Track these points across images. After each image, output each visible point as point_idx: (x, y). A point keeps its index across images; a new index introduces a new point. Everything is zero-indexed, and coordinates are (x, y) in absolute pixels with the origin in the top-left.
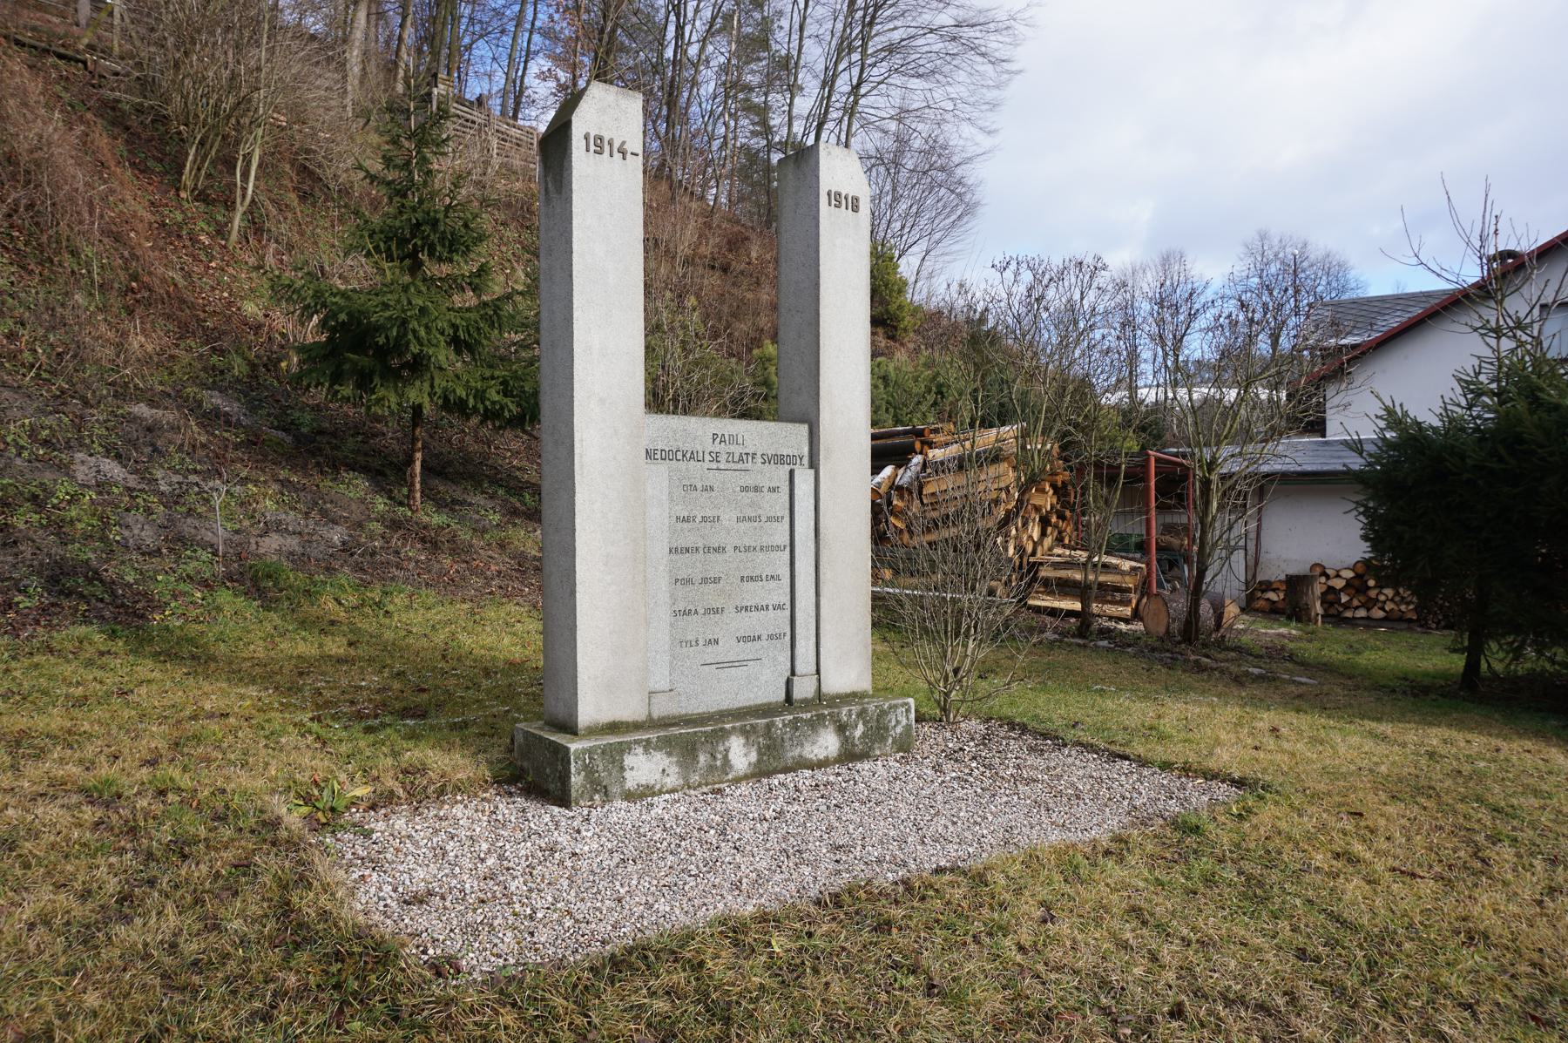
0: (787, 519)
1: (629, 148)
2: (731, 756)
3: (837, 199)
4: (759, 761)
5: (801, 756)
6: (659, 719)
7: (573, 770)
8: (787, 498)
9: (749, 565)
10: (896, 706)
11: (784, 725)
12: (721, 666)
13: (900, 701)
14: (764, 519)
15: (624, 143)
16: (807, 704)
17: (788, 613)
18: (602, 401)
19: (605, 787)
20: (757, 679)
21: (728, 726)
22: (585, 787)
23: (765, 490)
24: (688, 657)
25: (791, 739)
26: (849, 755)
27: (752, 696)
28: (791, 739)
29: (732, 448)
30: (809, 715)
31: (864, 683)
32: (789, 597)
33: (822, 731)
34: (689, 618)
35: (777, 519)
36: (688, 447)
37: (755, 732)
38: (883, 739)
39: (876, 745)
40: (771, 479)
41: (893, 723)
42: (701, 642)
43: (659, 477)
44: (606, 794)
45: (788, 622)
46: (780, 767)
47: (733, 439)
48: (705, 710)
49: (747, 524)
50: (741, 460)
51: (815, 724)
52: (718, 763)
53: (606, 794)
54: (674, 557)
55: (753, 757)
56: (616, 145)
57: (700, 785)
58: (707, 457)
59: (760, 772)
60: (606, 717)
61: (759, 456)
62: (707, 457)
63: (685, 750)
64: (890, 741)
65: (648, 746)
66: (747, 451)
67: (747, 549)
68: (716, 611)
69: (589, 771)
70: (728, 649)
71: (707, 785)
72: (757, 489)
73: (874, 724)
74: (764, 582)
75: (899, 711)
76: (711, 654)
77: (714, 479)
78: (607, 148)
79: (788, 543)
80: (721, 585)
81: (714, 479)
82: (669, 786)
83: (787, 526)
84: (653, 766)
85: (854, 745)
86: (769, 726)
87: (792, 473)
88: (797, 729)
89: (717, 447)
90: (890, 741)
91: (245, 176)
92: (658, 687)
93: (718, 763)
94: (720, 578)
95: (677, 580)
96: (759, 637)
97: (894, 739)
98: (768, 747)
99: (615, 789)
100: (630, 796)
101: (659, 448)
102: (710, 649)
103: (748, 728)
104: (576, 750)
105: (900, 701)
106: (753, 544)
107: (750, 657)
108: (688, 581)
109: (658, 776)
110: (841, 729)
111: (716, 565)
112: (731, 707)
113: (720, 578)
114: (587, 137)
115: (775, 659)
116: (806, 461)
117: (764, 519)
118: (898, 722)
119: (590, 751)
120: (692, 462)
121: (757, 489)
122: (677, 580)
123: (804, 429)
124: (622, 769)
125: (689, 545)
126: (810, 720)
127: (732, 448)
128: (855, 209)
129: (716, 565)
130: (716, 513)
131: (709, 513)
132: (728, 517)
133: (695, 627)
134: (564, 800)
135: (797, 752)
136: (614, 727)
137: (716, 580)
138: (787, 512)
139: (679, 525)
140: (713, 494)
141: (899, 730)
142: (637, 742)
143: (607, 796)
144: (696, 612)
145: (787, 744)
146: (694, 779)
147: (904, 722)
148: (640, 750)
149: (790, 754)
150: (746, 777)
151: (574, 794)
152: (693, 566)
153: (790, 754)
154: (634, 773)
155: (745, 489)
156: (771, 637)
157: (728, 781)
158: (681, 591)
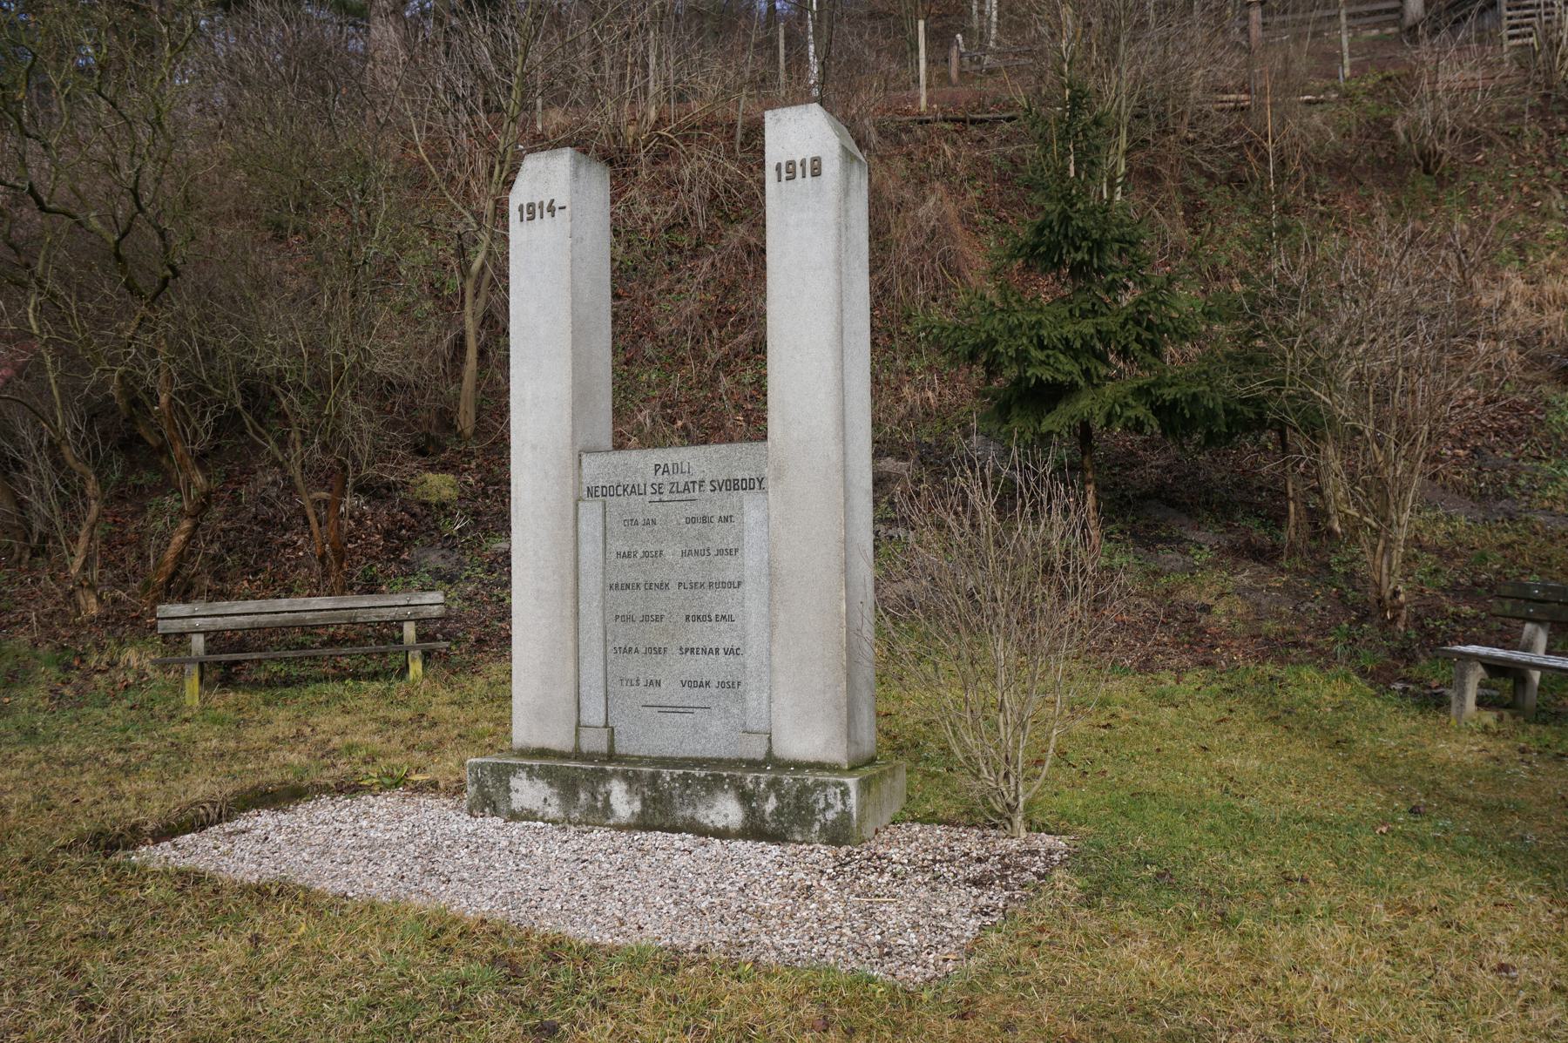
2: (612, 800)
9: (695, 603)
10: (825, 785)
11: (673, 779)
12: (663, 708)
13: (832, 779)
14: (713, 553)
15: (553, 201)
18: (534, 447)
20: (705, 729)
21: (609, 768)
23: (715, 520)
25: (680, 796)
26: (754, 830)
27: (699, 747)
28: (680, 796)
29: (677, 478)
30: (703, 774)
36: (629, 481)
37: (638, 781)
38: (807, 824)
39: (796, 828)
40: (722, 508)
41: (822, 805)
42: (642, 682)
43: (591, 512)
46: (667, 825)
47: (677, 468)
48: (646, 753)
49: (693, 559)
50: (686, 489)
51: (713, 785)
52: (599, 805)
54: (614, 593)
55: (637, 806)
56: (546, 206)
57: (580, 823)
58: (649, 490)
59: (643, 823)
60: (536, 741)
61: (707, 482)
62: (649, 490)
63: (567, 786)
64: (817, 827)
65: (531, 772)
66: (693, 479)
67: (694, 586)
68: (658, 651)
70: (670, 693)
72: (705, 519)
74: (714, 623)
75: (831, 791)
76: (652, 696)
77: (656, 511)
80: (663, 624)
81: (656, 511)
84: (536, 793)
85: (763, 821)
86: (655, 777)
88: (688, 786)
89: (660, 478)
90: (817, 827)
93: (599, 805)
94: (662, 616)
95: (617, 617)
96: (707, 684)
97: (824, 828)
98: (654, 800)
99: (502, 807)
101: (600, 484)
102: (651, 690)
103: (630, 774)
105: (832, 779)
106: (700, 580)
108: (628, 618)
109: (540, 804)
110: (745, 798)
111: (659, 603)
112: (674, 755)
113: (662, 616)
115: (726, 711)
117: (713, 553)
118: (829, 806)
119: (481, 766)
120: (633, 495)
121: (705, 519)
122: (617, 617)
124: (508, 790)
127: (677, 478)
128: (817, 172)
129: (659, 603)
131: (651, 548)
132: (672, 552)
133: (635, 666)
135: (688, 812)
137: (658, 618)
139: (620, 561)
140: (656, 527)
141: (831, 815)
142: (522, 767)
143: (495, 812)
145: (677, 801)
146: (576, 815)
147: (839, 807)
148: (524, 775)
149: (679, 813)
152: (628, 602)
153: (679, 813)
154: (519, 795)
155: (691, 520)
156: (722, 685)
157: (609, 826)
158: (621, 628)
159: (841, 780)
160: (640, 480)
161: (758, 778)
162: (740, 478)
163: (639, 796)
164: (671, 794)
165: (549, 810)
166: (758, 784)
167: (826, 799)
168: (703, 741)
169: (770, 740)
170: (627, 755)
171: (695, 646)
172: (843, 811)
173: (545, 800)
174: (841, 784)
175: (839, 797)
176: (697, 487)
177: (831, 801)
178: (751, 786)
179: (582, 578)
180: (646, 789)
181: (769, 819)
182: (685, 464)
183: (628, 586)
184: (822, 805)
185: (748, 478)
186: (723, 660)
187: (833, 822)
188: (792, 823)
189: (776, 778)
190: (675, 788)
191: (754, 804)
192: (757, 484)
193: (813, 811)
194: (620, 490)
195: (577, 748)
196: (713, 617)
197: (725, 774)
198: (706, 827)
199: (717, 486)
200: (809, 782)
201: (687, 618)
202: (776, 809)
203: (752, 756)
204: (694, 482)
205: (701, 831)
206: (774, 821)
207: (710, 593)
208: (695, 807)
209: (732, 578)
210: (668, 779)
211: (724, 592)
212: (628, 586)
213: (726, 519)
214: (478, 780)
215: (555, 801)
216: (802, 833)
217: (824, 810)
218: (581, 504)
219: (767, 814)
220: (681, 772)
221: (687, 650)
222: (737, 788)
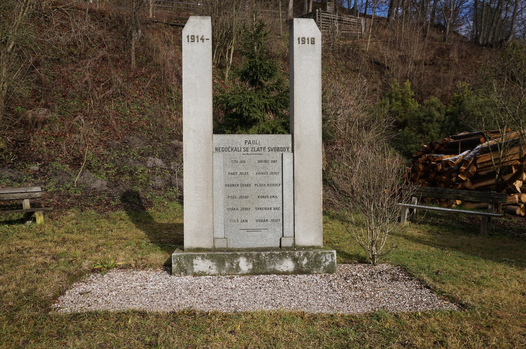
1: (205, 38)
2: (240, 265)
3: (303, 41)
4: (253, 268)
5: (274, 269)
6: (218, 248)
7: (173, 262)
9: (262, 191)
10: (325, 253)
11: (266, 255)
12: (248, 230)
13: (328, 251)
15: (203, 36)
16: (288, 248)
18: (194, 131)
19: (185, 270)
20: (266, 237)
22: (177, 269)
23: (270, 162)
24: (234, 226)
26: (299, 271)
27: (263, 243)
29: (254, 146)
30: (278, 253)
31: (319, 242)
33: (285, 260)
34: (234, 211)
36: (234, 146)
38: (318, 267)
39: (314, 269)
40: (273, 157)
41: (324, 260)
42: (239, 221)
43: (219, 158)
44: (186, 272)
46: (263, 272)
47: (254, 142)
48: (241, 247)
50: (258, 150)
51: (283, 256)
52: (234, 267)
53: (186, 272)
54: (227, 188)
55: (251, 266)
56: (200, 38)
57: (226, 274)
58: (243, 150)
59: (253, 273)
60: (195, 245)
61: (267, 148)
62: (243, 150)
63: (220, 261)
64: (322, 268)
65: (203, 257)
67: (261, 185)
68: (246, 209)
69: (179, 263)
70: (252, 224)
71: (229, 275)
72: (265, 161)
73: (313, 260)
75: (327, 255)
76: (244, 225)
77: (246, 158)
78: (196, 39)
80: (248, 199)
81: (246, 158)
82: (212, 273)
84: (205, 265)
85: (302, 267)
86: (258, 256)
87: (282, 154)
88: (272, 258)
89: (247, 145)
90: (322, 268)
91: (229, 56)
92: (219, 237)
93: (234, 267)
94: (248, 197)
96: (267, 220)
97: (325, 268)
98: (258, 263)
99: (189, 271)
100: (195, 275)
101: (221, 147)
102: (243, 223)
104: (174, 255)
108: (234, 197)
109: (208, 269)
110: (295, 260)
111: (247, 191)
112: (253, 247)
113: (248, 197)
114: (188, 37)
115: (274, 230)
116: (290, 149)
118: (326, 260)
119: (180, 256)
121: (265, 161)
122: (229, 197)
123: (290, 135)
124: (192, 264)
125: (234, 183)
126: (278, 255)
127: (254, 146)
128: (313, 43)
129: (247, 191)
130: (246, 171)
131: (243, 171)
132: (252, 173)
133: (236, 215)
134: (170, 273)
135: (272, 267)
136: (198, 250)
137: (247, 197)
139: (230, 176)
141: (327, 263)
142: (198, 255)
143: (186, 274)
144: (237, 209)
145: (267, 263)
146: (224, 272)
147: (330, 260)
148: (200, 258)
149: (268, 268)
150: (247, 274)
151: (173, 271)
153: (268, 268)
154: (197, 266)
155: (260, 161)
156: (273, 221)
158: (230, 201)
159: (331, 251)
160: (239, 146)
161: (300, 253)
162: (280, 147)
163: (252, 263)
164: (265, 261)
165: (212, 271)
166: (300, 255)
167: (326, 258)
168: (265, 241)
169: (294, 240)
170: (233, 248)
171: (262, 207)
172: (332, 262)
173: (210, 267)
174: (331, 253)
175: (330, 257)
177: (328, 258)
178: (297, 256)
179: (215, 182)
180: (254, 260)
181: (304, 267)
183: (233, 185)
184: (324, 260)
186: (273, 212)
187: (328, 265)
188: (313, 267)
189: (307, 252)
190: (267, 258)
191: (298, 262)
192: (287, 150)
193: (321, 262)
194: (230, 149)
195: (214, 246)
196: (269, 196)
197: (287, 252)
198: (279, 271)
199: (271, 150)
200: (319, 253)
201: (259, 197)
202: (307, 263)
203: (287, 245)
204: (261, 148)
205: (279, 273)
206: (306, 267)
207: (268, 188)
208: (275, 265)
209: (277, 183)
210: (264, 255)
212: (233, 185)
214: (178, 262)
215: (214, 267)
216: (316, 270)
217: (325, 262)
218: (214, 154)
219: (303, 265)
220: (269, 253)
222: (292, 257)
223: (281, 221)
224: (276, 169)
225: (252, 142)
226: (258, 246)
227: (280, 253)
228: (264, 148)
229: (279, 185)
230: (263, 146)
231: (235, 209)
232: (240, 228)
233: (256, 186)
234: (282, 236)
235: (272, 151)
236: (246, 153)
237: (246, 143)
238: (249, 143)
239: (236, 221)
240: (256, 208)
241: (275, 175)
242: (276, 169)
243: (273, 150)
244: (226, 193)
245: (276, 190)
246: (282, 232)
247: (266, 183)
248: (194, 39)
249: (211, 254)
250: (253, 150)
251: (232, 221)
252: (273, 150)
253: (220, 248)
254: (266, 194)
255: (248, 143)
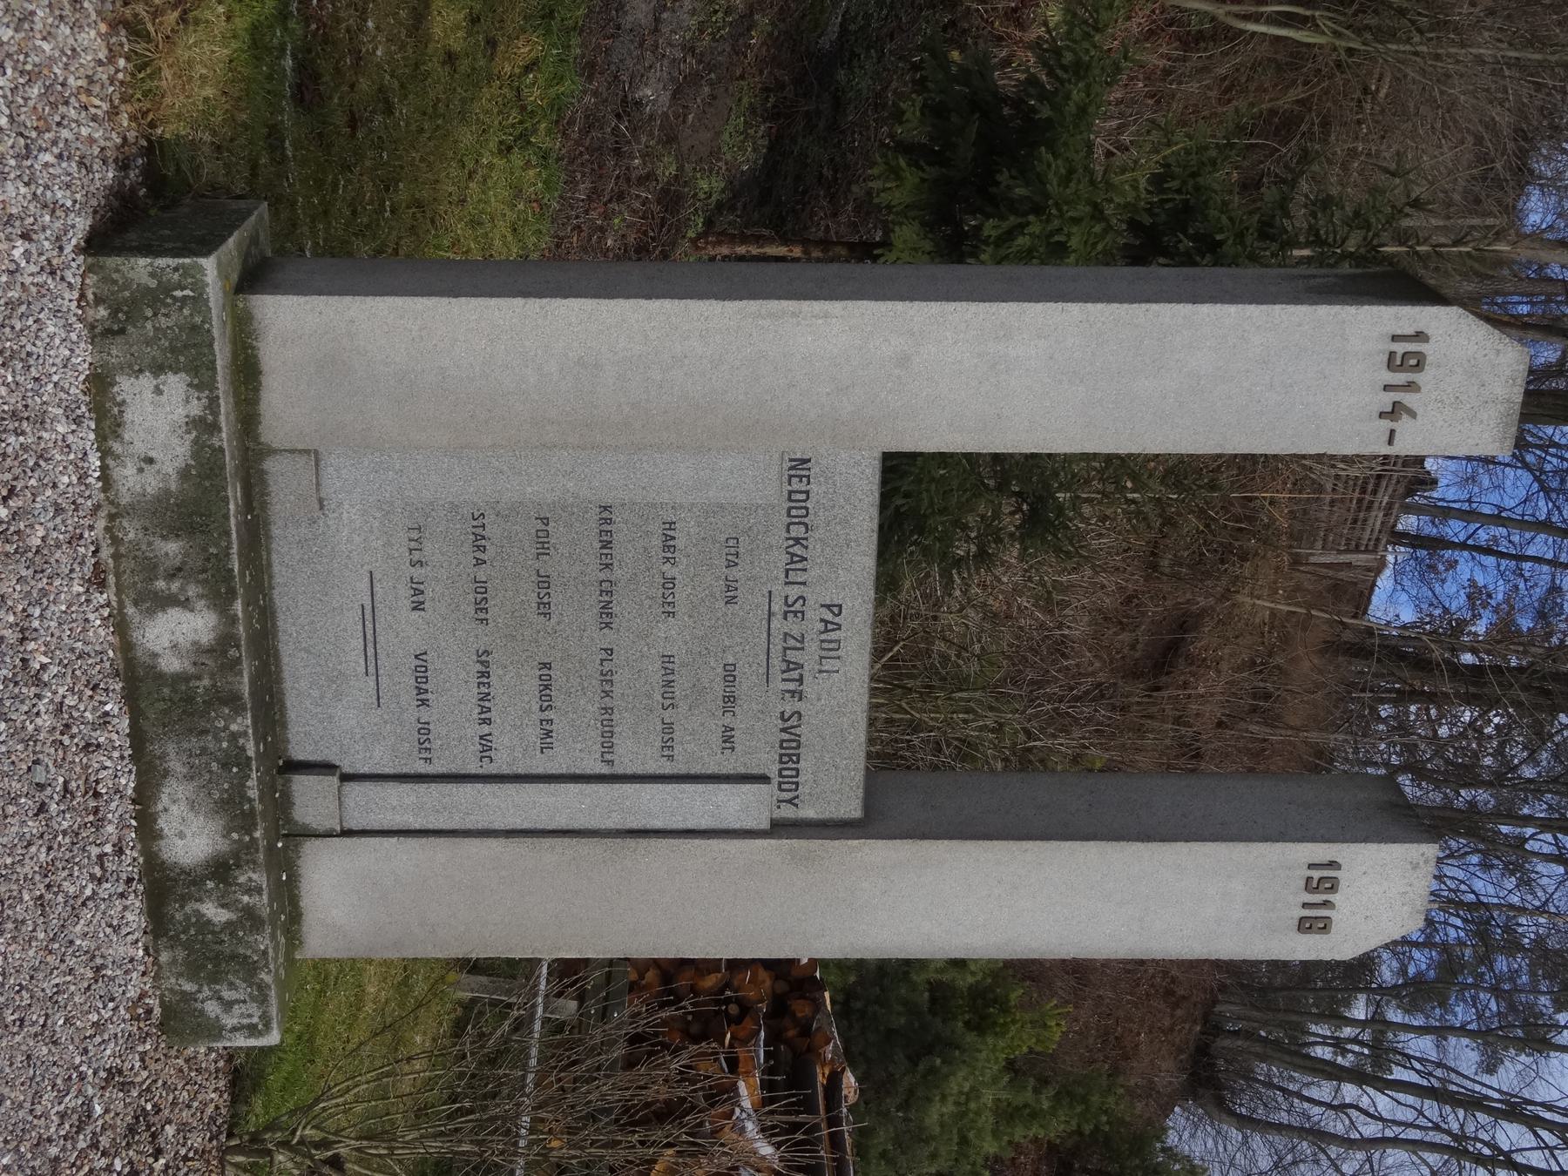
0: (668, 768)
1: (1404, 425)
2: (174, 614)
3: (1323, 882)
4: (160, 677)
5: (166, 774)
6: (263, 472)
7: (162, 262)
8: (712, 769)
10: (263, 1000)
11: (234, 737)
13: (274, 1011)
14: (668, 715)
15: (1413, 414)
16: (281, 805)
17: (473, 768)
18: (903, 361)
19: (122, 331)
21: (238, 606)
22: (126, 286)
23: (728, 719)
24: (388, 544)
25: (204, 750)
27: (303, 685)
28: (204, 750)
29: (812, 647)
30: (253, 793)
31: (318, 942)
32: (506, 770)
33: (217, 824)
34: (467, 547)
35: (667, 745)
36: (815, 550)
37: (222, 667)
38: (193, 970)
39: (181, 954)
41: (227, 994)
42: (418, 572)
44: (108, 332)
45: (453, 768)
47: (830, 649)
48: (278, 580)
49: (657, 678)
50: (790, 666)
51: (234, 812)
52: (161, 584)
53: (108, 332)
54: (593, 515)
55: (171, 664)
56: (1408, 399)
57: (116, 541)
58: (794, 592)
60: (273, 356)
61: (799, 706)
62: (794, 592)
64: (189, 987)
65: (203, 426)
67: (607, 678)
68: (481, 607)
69: (158, 296)
71: (116, 557)
72: (730, 700)
73: (226, 948)
75: (254, 1010)
78: (1400, 378)
79: (619, 770)
82: (117, 473)
83: (652, 767)
85: (184, 900)
87: (763, 779)
88: (225, 766)
89: (814, 614)
90: (189, 987)
91: (1274, 20)
92: (329, 472)
93: (161, 584)
95: (545, 521)
96: (424, 702)
97: (187, 997)
98: (189, 699)
99: (117, 352)
100: (99, 383)
101: (813, 487)
102: (405, 592)
103: (233, 652)
104: (201, 270)
105: (274, 1011)
106: (617, 690)
107: (383, 680)
108: (543, 547)
109: (140, 448)
110: (220, 870)
112: (282, 637)
114: (1420, 336)
116: (788, 812)
117: (668, 715)
118: (228, 1006)
119: (199, 301)
120: (785, 558)
121: (730, 700)
122: (545, 521)
123: (852, 808)
124: (158, 369)
126: (245, 798)
127: (812, 647)
128: (1310, 925)
130: (681, 608)
131: (681, 594)
132: (672, 635)
134: (97, 244)
135: (176, 765)
136: (248, 372)
137: (544, 608)
138: (681, 768)
139: (656, 528)
141: (212, 1008)
142: (213, 404)
143: (101, 335)
144: (480, 562)
145: (194, 743)
146: (131, 531)
147: (229, 1021)
148: (196, 409)
149: (171, 748)
150: (127, 647)
151: (111, 262)
153: (171, 748)
154: (148, 395)
155: (730, 674)
156: (424, 729)
157: (121, 603)
159: (275, 1025)
160: (813, 573)
161: (259, 890)
163: (192, 670)
164: (205, 732)
165: (130, 470)
166: (249, 891)
167: (237, 1001)
168: (315, 693)
169: (329, 834)
171: (493, 679)
172: (222, 1028)
173: (150, 461)
174: (267, 1026)
175: (245, 1021)
176: (792, 686)
177: (236, 1009)
178: (242, 879)
180: (206, 682)
181: (188, 909)
182: (836, 664)
183: (606, 545)
184: (227, 994)
185: (801, 779)
187: (202, 1012)
188: (187, 946)
189: (262, 923)
190: (218, 740)
191: (210, 884)
193: (216, 982)
194: (799, 531)
195: (272, 452)
197: (257, 834)
198: (155, 798)
199: (790, 725)
200: (263, 976)
201: (546, 665)
202: (209, 922)
204: (800, 680)
205: (144, 799)
206: (187, 917)
207: (594, 708)
208: (190, 778)
210: (234, 727)
211: (594, 734)
212: (606, 545)
213: (728, 739)
214: (167, 289)
215: (152, 483)
216: (174, 962)
217: (220, 998)
219: (197, 906)
221: (485, 664)
222: (236, 855)
223: (422, 768)
224: (690, 747)
225: (833, 636)
226: (285, 660)
227: (250, 800)
228: (798, 695)
229: (610, 762)
230: (807, 688)
231: (483, 549)
232: (377, 576)
233: (605, 656)
234: (347, 769)
235: (783, 730)
236: (778, 607)
237: (828, 607)
238: (826, 622)
239: (416, 556)
240: (486, 652)
241: (658, 744)
242: (690, 747)
243: (787, 736)
244: (564, 509)
245: (579, 746)
246: (365, 770)
247: (616, 702)
248: (1402, 367)
249: (223, 467)
250: (792, 643)
251: (415, 535)
252: (787, 736)
253: (263, 482)
254: (558, 699)
255: (829, 617)
